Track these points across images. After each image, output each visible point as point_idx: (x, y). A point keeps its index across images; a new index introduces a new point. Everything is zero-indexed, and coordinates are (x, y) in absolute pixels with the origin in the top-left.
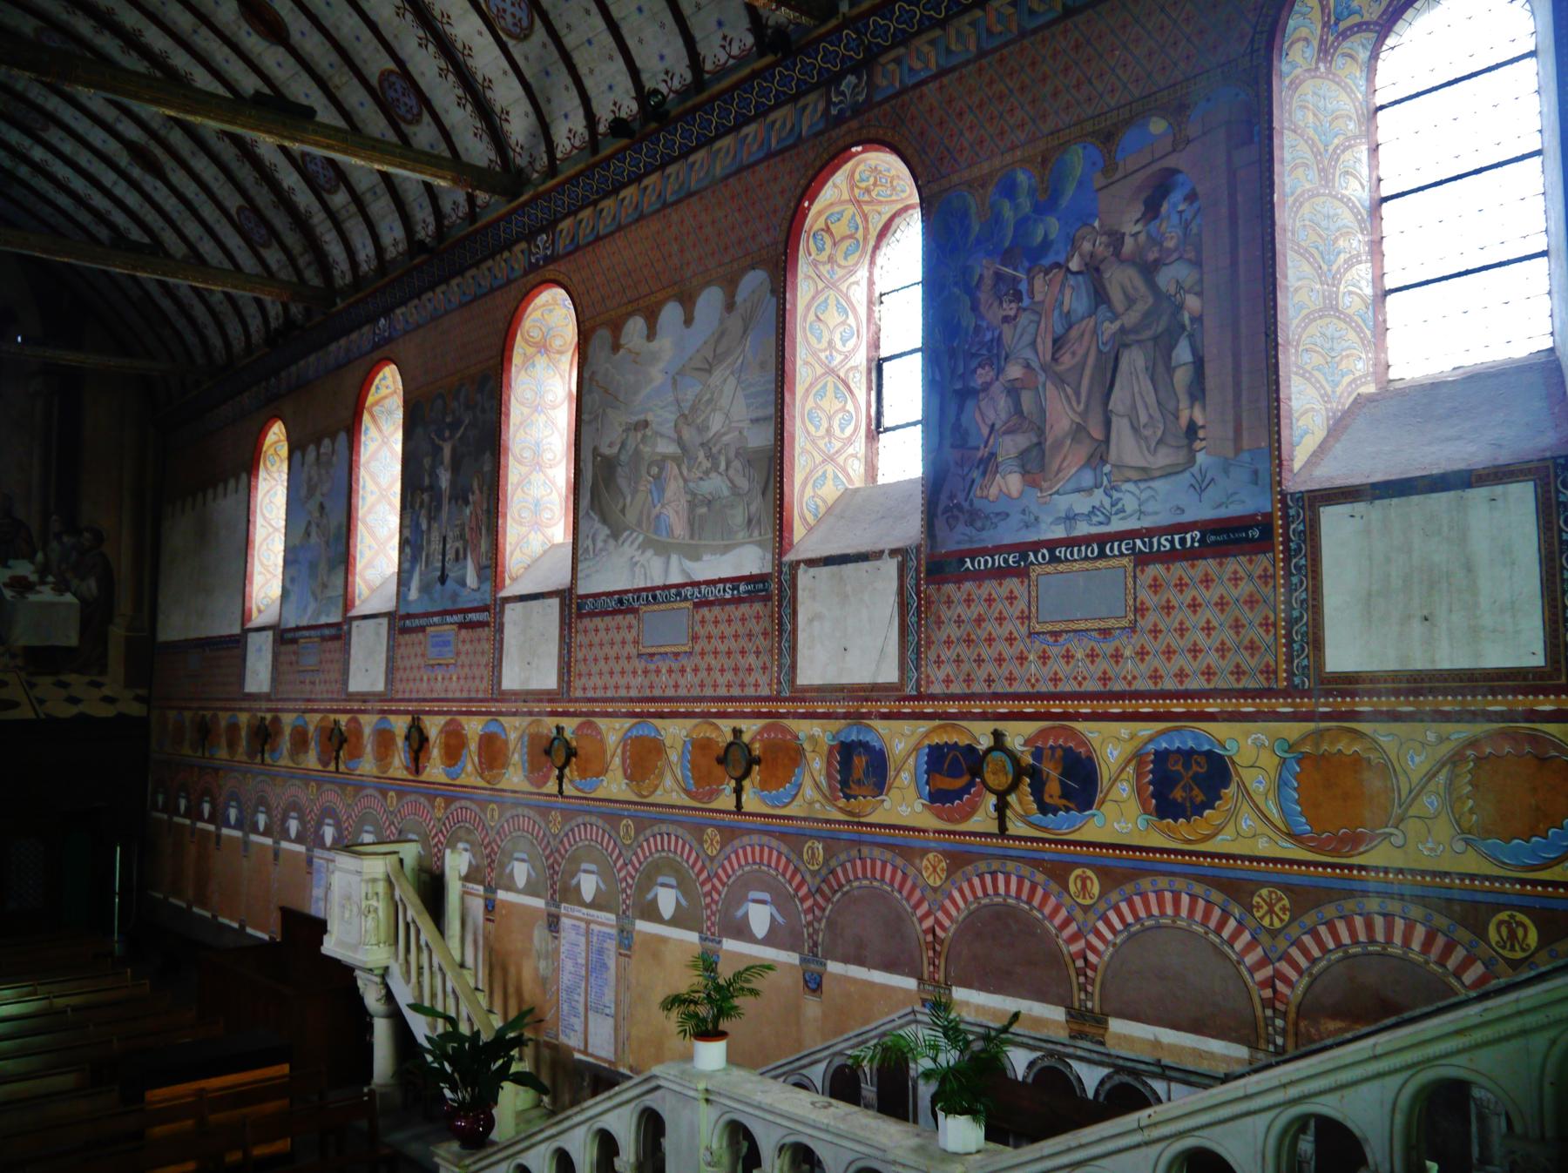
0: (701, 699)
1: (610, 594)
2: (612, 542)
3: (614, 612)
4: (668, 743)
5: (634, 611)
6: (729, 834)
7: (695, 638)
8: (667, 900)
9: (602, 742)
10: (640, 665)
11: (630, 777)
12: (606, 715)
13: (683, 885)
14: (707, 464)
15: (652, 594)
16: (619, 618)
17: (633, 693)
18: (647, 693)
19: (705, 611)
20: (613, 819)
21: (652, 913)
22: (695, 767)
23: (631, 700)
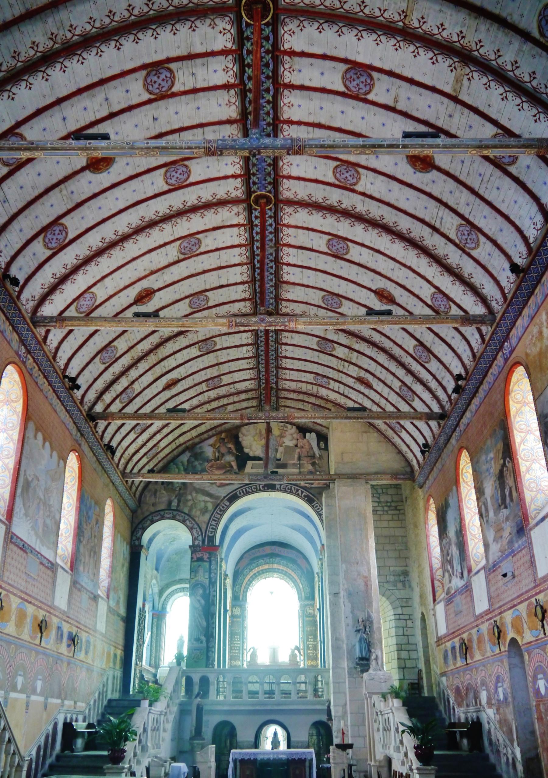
0: (37, 599)
1: (22, 540)
2: (24, 517)
3: (21, 549)
4: (28, 614)
5: (27, 553)
6: (37, 652)
7: (38, 575)
8: (20, 680)
9: (11, 606)
10: (24, 576)
11: (17, 626)
12: (15, 595)
13: (24, 676)
14: (48, 513)
15: (33, 550)
16: (19, 550)
17: (22, 588)
18: (25, 590)
19: (41, 566)
20: (9, 643)
21: (14, 688)
22: (33, 626)
23: (21, 591)
